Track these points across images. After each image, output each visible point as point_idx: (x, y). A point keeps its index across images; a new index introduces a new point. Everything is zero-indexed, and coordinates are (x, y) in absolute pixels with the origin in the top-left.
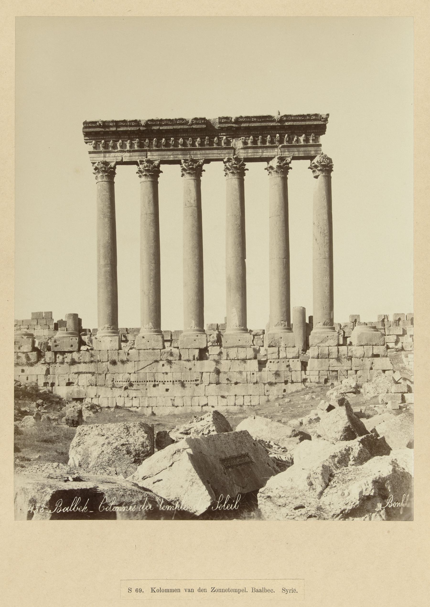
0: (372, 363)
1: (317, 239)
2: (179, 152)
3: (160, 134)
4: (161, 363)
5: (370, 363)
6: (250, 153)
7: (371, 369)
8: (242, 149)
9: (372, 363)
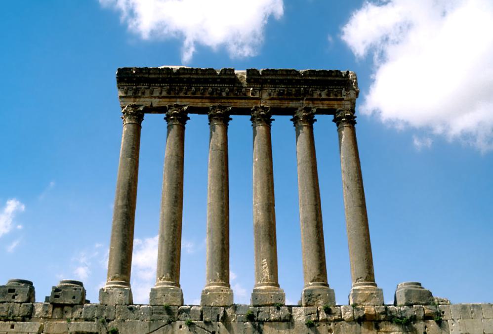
1: (349, 187)
2: (207, 101)
3: (190, 82)
6: (277, 103)
8: (268, 99)
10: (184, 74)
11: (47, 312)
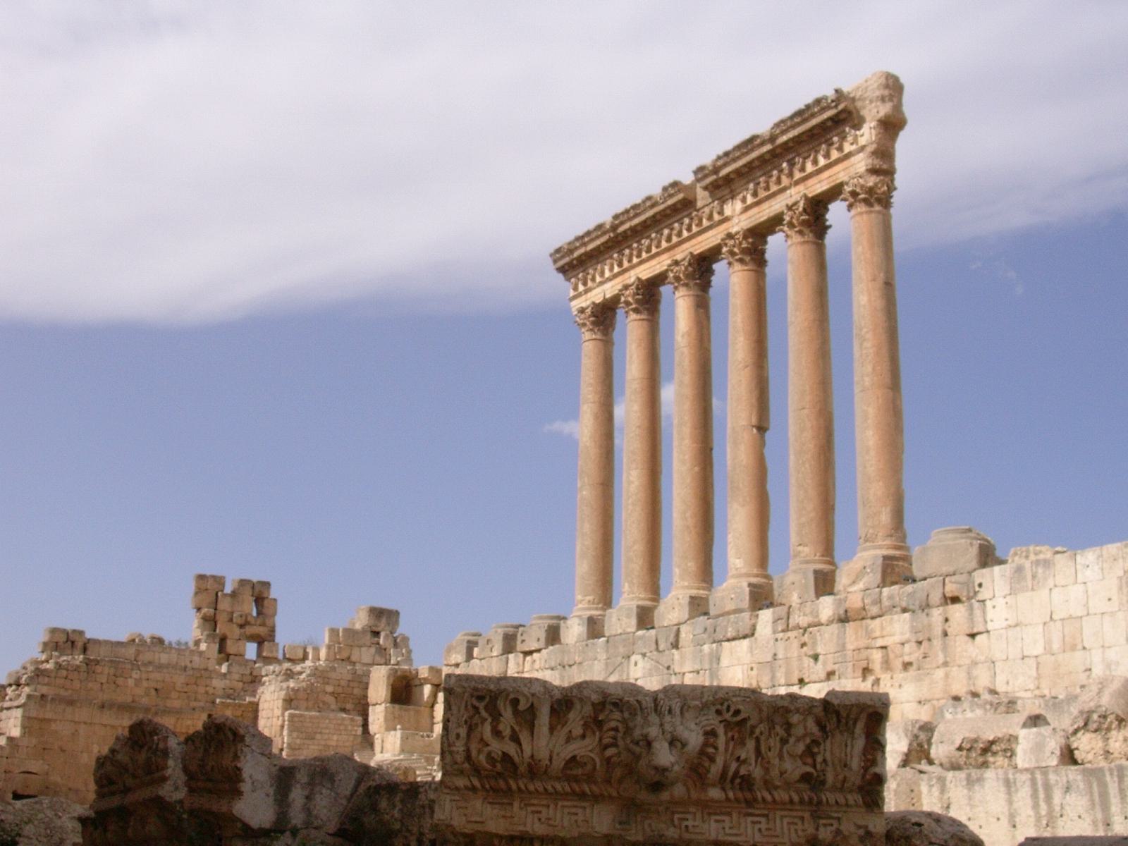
0: (947, 620)
4: (634, 658)
5: (941, 619)
7: (946, 634)
9: (947, 620)
10: (622, 223)
11: (518, 664)
